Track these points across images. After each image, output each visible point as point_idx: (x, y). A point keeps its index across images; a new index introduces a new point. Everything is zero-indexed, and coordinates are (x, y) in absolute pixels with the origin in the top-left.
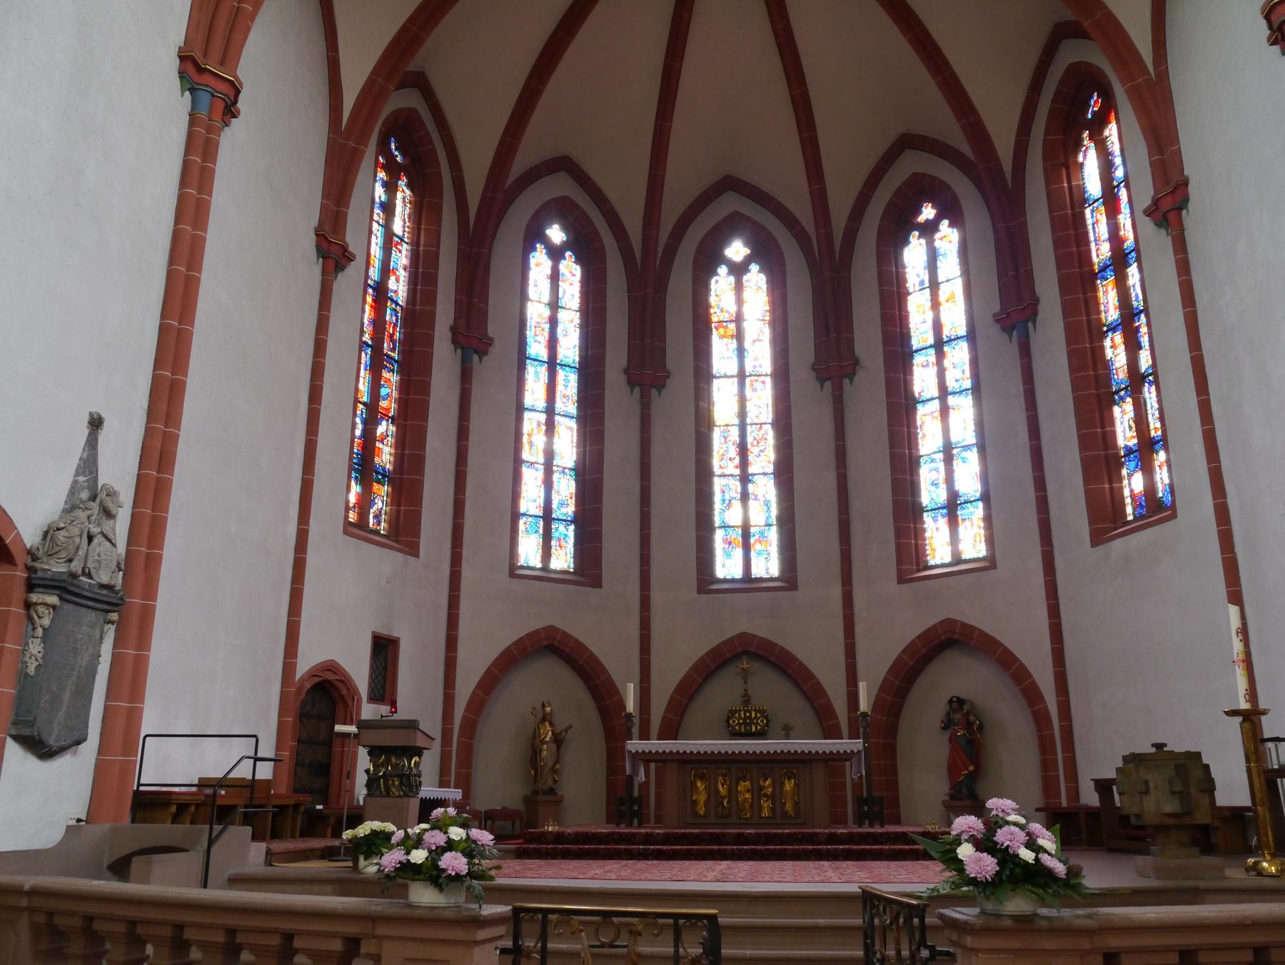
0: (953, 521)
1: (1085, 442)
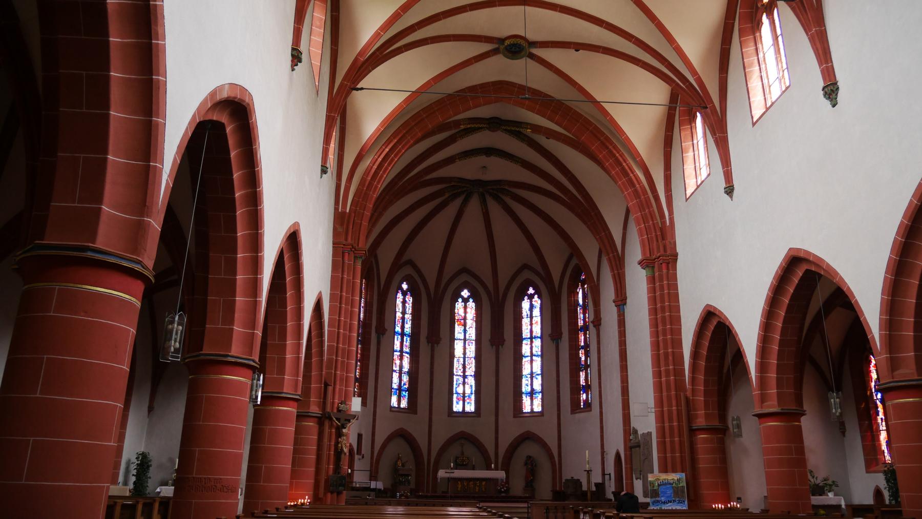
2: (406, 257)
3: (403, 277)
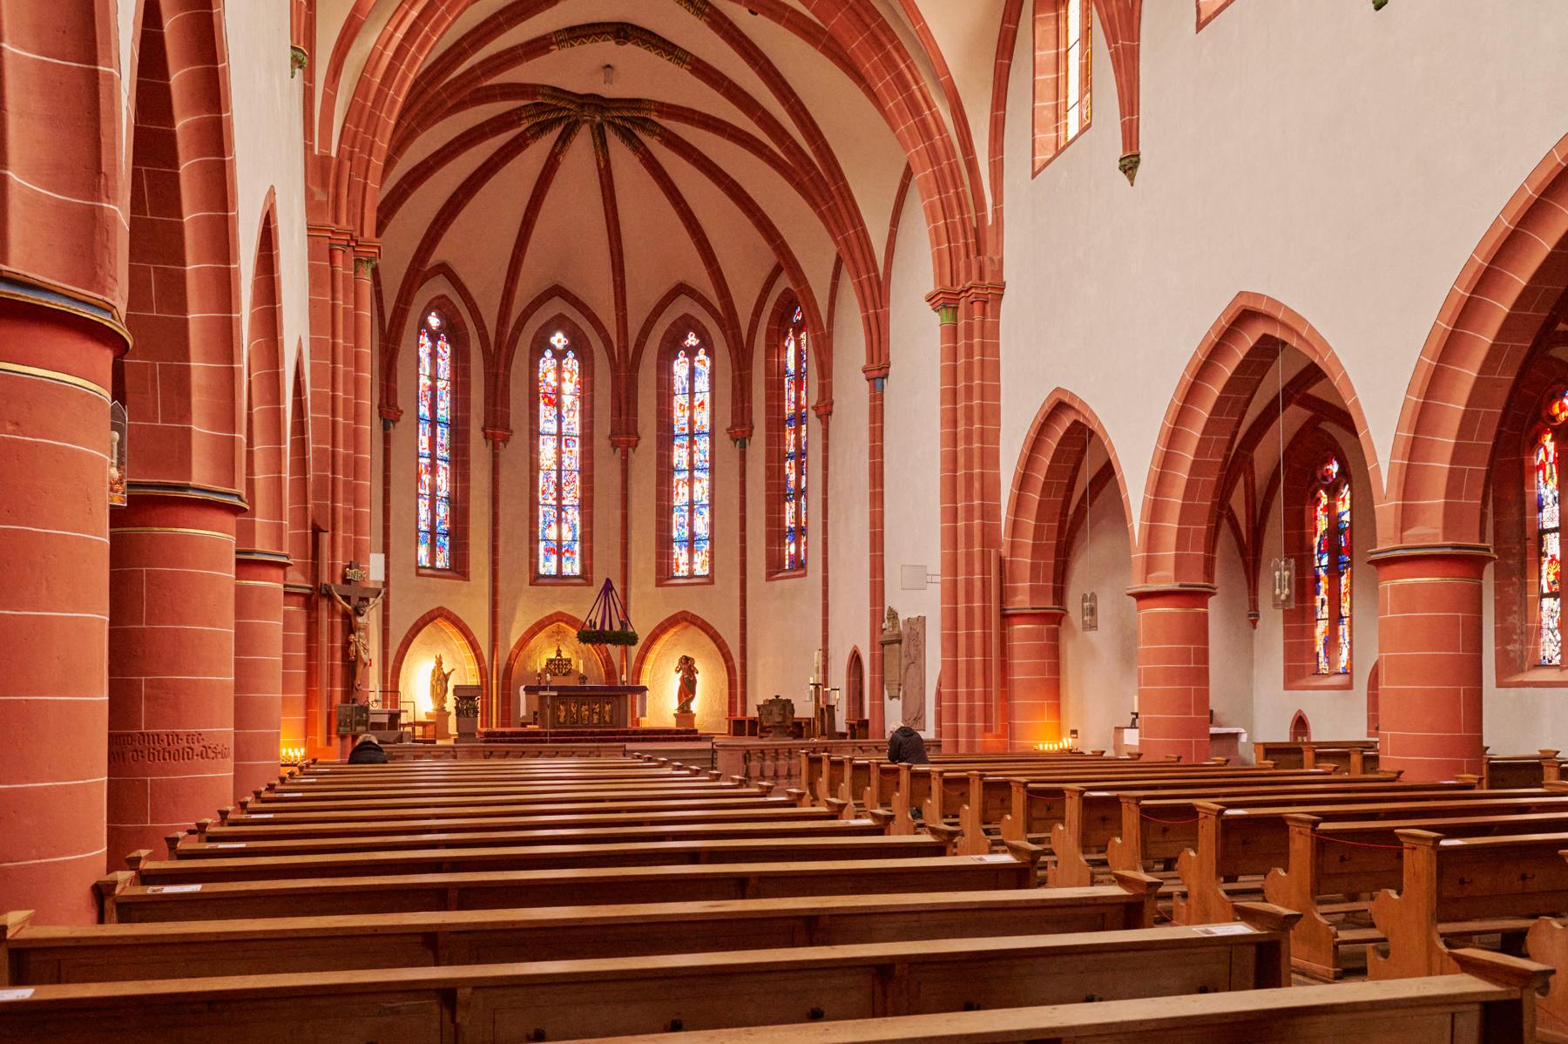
0: (691, 552)
2: (437, 257)
3: (431, 302)
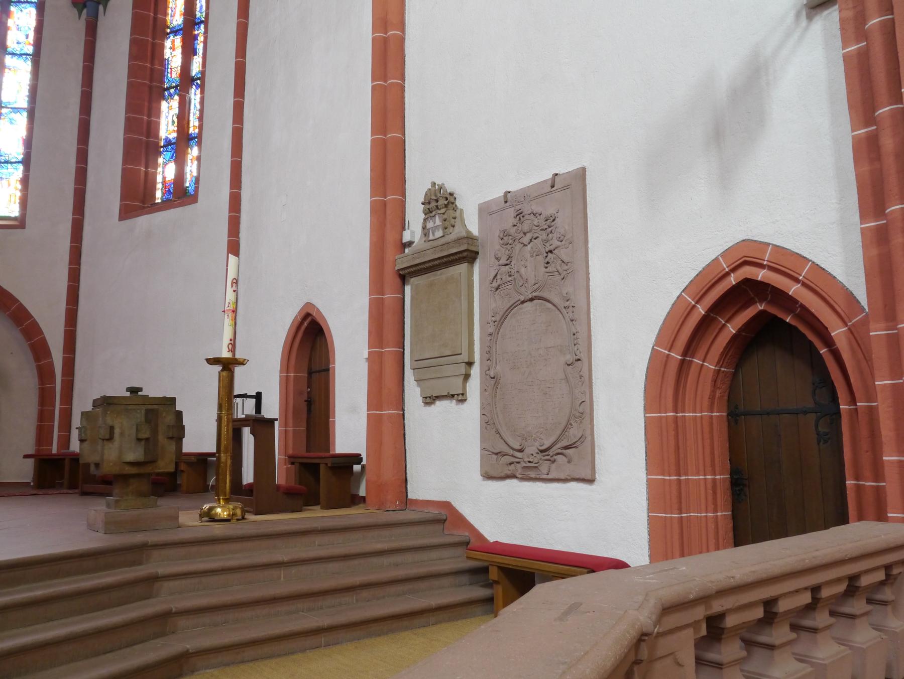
1: (131, 125)
